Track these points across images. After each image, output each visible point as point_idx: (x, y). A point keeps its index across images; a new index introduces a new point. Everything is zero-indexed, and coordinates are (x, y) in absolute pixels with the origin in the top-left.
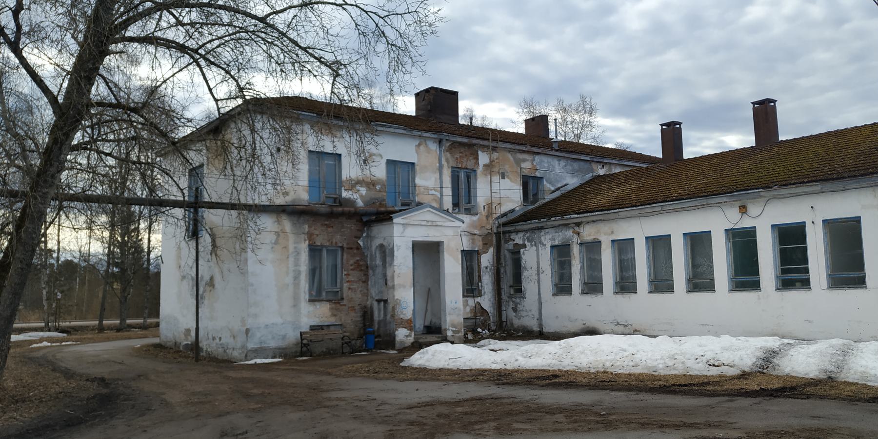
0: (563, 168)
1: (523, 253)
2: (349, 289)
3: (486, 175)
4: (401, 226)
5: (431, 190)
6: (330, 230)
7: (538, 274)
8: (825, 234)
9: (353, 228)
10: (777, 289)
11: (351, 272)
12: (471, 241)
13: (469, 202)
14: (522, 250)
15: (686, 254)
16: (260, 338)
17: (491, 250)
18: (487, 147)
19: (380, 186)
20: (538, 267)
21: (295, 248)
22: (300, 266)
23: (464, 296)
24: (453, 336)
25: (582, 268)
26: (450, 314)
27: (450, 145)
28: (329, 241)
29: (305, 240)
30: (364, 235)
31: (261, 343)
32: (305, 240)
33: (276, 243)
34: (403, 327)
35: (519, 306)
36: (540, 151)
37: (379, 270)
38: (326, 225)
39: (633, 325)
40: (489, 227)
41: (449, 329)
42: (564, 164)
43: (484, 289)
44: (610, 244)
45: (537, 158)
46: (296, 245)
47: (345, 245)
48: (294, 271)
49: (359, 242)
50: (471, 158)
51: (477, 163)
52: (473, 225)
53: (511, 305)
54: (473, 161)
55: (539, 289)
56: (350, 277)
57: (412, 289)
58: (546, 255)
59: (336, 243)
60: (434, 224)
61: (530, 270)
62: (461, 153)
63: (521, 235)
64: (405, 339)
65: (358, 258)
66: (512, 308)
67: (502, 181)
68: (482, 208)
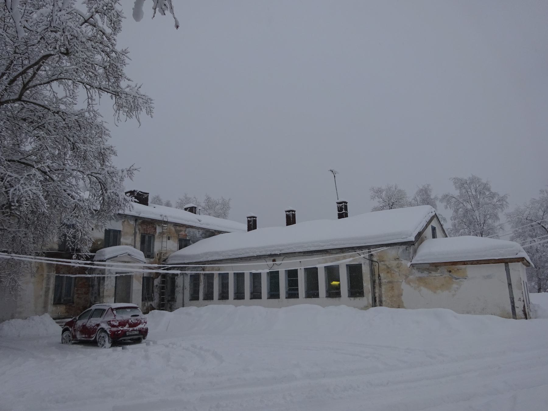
1: (177, 279)
2: (78, 298)
3: (160, 238)
7: (183, 289)
8: (305, 274)
10: (286, 298)
13: (150, 251)
14: (176, 277)
15: (251, 281)
20: (184, 286)
21: (48, 275)
23: (142, 300)
25: (204, 287)
27: (141, 222)
29: (54, 271)
32: (54, 271)
35: (172, 306)
37: (96, 287)
44: (218, 275)
48: (46, 288)
49: (86, 272)
51: (155, 231)
53: (169, 305)
55: (183, 297)
57: (114, 298)
58: (188, 280)
61: (179, 287)
62: (147, 226)
65: (85, 281)
66: (169, 307)
67: (168, 241)
68: (157, 254)
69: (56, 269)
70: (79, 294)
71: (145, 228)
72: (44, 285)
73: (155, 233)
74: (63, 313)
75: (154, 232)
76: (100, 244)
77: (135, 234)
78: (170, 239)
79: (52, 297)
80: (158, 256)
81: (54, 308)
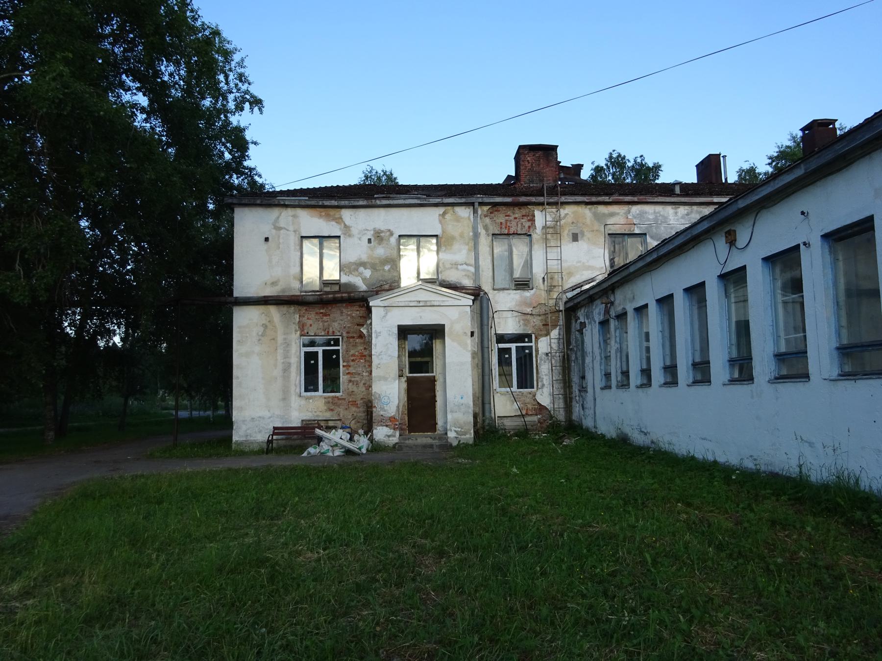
0: (683, 217)
2: (350, 381)
4: (382, 309)
5: (462, 264)
6: (325, 318)
9: (354, 315)
11: (352, 363)
16: (246, 431)
17: (555, 333)
18: (542, 204)
19: (389, 266)
20: (593, 352)
21: (285, 339)
24: (456, 437)
26: (452, 412)
28: (325, 330)
29: (296, 331)
30: (369, 322)
31: (247, 436)
33: (262, 336)
36: (636, 199)
39: (651, 434)
40: (552, 302)
41: (451, 430)
42: (686, 212)
43: (542, 381)
45: (635, 209)
46: (285, 337)
47: (345, 334)
48: (283, 363)
49: (361, 330)
50: (522, 220)
52: (525, 303)
54: (528, 224)
57: (397, 381)
59: (333, 332)
62: (506, 216)
63: (582, 311)
64: (386, 439)
68: (541, 281)
69: (299, 327)
71: (501, 223)
72: (280, 358)
73: (531, 230)
75: (529, 227)
76: (389, 270)
77: (476, 236)
78: (579, 238)
79: (296, 381)
80: (546, 282)
81: (303, 402)
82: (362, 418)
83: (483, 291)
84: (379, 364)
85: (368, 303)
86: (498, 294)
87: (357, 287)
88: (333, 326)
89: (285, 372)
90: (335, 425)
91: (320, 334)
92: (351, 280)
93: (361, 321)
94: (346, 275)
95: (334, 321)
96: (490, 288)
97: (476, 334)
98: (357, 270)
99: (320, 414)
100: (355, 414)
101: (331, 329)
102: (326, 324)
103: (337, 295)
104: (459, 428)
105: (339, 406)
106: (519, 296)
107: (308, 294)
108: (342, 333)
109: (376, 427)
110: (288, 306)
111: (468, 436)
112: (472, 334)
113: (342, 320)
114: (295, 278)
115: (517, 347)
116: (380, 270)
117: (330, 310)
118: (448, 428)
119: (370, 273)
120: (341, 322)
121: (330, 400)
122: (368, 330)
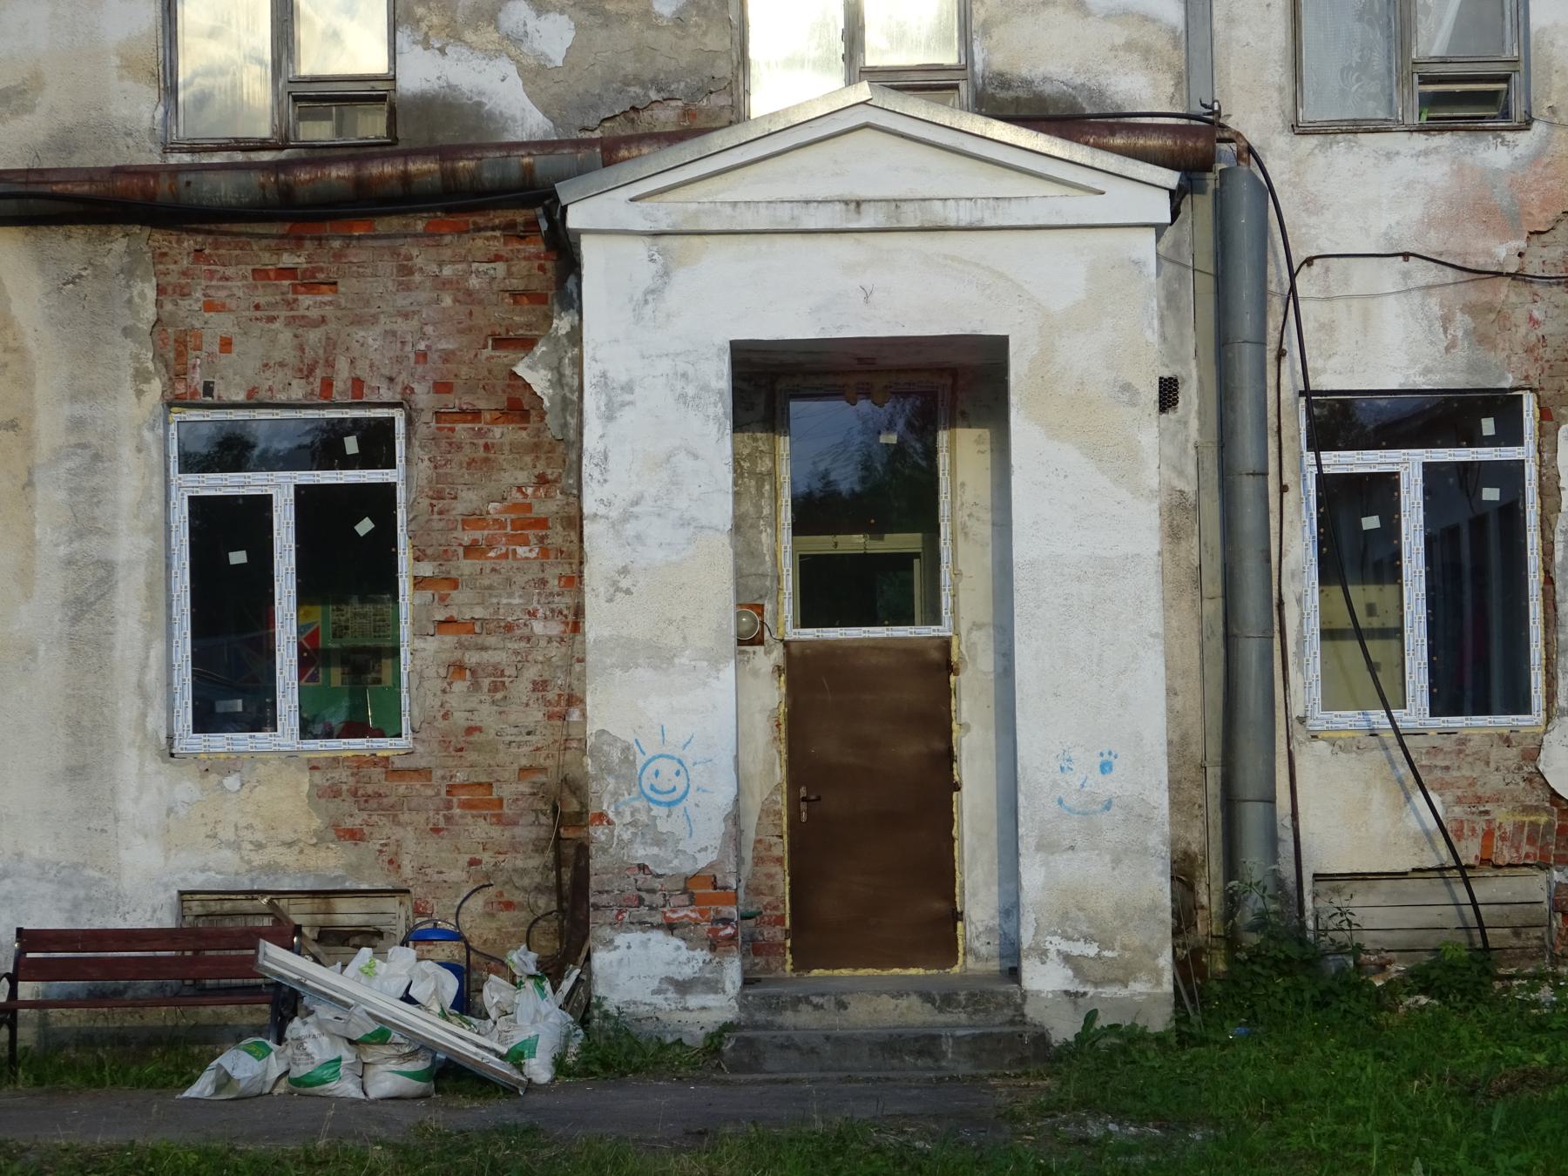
2: (458, 668)
4: (640, 247)
6: (306, 300)
9: (474, 282)
11: (466, 567)
12: (1462, 321)
21: (77, 424)
22: (109, 534)
26: (1046, 846)
28: (307, 373)
29: (141, 376)
30: (562, 325)
34: (643, 925)
38: (289, 272)
41: (1043, 955)
46: (79, 410)
47: (423, 397)
48: (70, 562)
49: (520, 370)
56: (458, 596)
57: (729, 672)
59: (358, 384)
60: (911, 217)
64: (666, 1003)
69: (159, 356)
70: (468, 626)
74: (290, 845)
79: (144, 667)
81: (187, 789)
82: (526, 882)
83: (1236, 137)
84: (624, 571)
85: (556, 214)
86: (1320, 160)
87: (490, 116)
88: (356, 351)
89: (73, 625)
90: (377, 921)
91: (281, 397)
92: (454, 81)
93: (520, 318)
94: (427, 45)
95: (358, 321)
96: (1276, 120)
97: (1189, 396)
98: (493, 19)
99: (287, 858)
100: (486, 857)
101: (342, 365)
102: (314, 336)
103: (375, 169)
104: (1088, 939)
105: (392, 812)
106: (1446, 168)
107: (206, 159)
108: (408, 389)
109: (607, 932)
110: (94, 231)
111: (1139, 987)
112: (1168, 393)
113: (406, 316)
114: (129, 65)
115: (1428, 468)
116: (624, 18)
117: (338, 256)
118: (1027, 938)
119: (569, 37)
120: (401, 326)
121: (343, 775)
122: (558, 370)
